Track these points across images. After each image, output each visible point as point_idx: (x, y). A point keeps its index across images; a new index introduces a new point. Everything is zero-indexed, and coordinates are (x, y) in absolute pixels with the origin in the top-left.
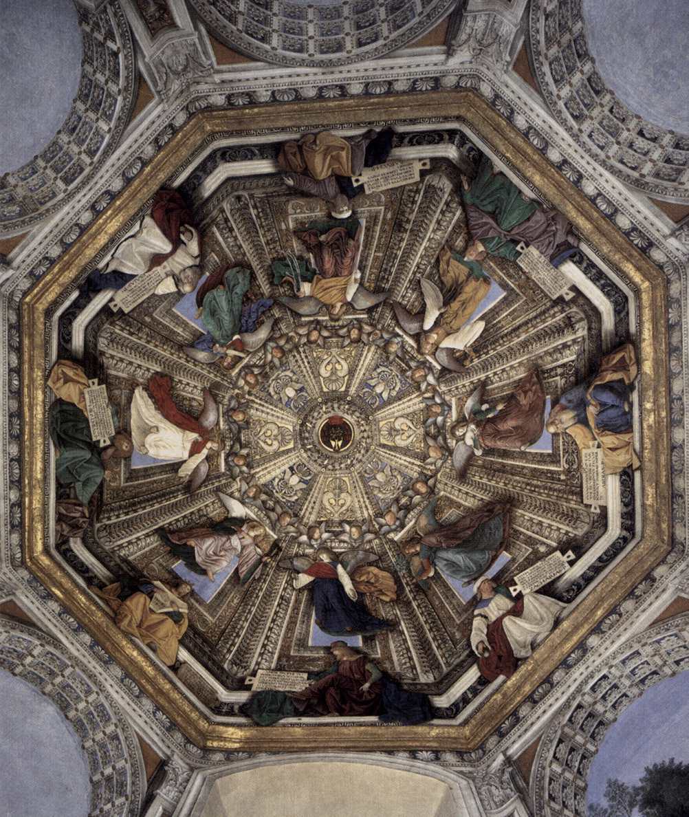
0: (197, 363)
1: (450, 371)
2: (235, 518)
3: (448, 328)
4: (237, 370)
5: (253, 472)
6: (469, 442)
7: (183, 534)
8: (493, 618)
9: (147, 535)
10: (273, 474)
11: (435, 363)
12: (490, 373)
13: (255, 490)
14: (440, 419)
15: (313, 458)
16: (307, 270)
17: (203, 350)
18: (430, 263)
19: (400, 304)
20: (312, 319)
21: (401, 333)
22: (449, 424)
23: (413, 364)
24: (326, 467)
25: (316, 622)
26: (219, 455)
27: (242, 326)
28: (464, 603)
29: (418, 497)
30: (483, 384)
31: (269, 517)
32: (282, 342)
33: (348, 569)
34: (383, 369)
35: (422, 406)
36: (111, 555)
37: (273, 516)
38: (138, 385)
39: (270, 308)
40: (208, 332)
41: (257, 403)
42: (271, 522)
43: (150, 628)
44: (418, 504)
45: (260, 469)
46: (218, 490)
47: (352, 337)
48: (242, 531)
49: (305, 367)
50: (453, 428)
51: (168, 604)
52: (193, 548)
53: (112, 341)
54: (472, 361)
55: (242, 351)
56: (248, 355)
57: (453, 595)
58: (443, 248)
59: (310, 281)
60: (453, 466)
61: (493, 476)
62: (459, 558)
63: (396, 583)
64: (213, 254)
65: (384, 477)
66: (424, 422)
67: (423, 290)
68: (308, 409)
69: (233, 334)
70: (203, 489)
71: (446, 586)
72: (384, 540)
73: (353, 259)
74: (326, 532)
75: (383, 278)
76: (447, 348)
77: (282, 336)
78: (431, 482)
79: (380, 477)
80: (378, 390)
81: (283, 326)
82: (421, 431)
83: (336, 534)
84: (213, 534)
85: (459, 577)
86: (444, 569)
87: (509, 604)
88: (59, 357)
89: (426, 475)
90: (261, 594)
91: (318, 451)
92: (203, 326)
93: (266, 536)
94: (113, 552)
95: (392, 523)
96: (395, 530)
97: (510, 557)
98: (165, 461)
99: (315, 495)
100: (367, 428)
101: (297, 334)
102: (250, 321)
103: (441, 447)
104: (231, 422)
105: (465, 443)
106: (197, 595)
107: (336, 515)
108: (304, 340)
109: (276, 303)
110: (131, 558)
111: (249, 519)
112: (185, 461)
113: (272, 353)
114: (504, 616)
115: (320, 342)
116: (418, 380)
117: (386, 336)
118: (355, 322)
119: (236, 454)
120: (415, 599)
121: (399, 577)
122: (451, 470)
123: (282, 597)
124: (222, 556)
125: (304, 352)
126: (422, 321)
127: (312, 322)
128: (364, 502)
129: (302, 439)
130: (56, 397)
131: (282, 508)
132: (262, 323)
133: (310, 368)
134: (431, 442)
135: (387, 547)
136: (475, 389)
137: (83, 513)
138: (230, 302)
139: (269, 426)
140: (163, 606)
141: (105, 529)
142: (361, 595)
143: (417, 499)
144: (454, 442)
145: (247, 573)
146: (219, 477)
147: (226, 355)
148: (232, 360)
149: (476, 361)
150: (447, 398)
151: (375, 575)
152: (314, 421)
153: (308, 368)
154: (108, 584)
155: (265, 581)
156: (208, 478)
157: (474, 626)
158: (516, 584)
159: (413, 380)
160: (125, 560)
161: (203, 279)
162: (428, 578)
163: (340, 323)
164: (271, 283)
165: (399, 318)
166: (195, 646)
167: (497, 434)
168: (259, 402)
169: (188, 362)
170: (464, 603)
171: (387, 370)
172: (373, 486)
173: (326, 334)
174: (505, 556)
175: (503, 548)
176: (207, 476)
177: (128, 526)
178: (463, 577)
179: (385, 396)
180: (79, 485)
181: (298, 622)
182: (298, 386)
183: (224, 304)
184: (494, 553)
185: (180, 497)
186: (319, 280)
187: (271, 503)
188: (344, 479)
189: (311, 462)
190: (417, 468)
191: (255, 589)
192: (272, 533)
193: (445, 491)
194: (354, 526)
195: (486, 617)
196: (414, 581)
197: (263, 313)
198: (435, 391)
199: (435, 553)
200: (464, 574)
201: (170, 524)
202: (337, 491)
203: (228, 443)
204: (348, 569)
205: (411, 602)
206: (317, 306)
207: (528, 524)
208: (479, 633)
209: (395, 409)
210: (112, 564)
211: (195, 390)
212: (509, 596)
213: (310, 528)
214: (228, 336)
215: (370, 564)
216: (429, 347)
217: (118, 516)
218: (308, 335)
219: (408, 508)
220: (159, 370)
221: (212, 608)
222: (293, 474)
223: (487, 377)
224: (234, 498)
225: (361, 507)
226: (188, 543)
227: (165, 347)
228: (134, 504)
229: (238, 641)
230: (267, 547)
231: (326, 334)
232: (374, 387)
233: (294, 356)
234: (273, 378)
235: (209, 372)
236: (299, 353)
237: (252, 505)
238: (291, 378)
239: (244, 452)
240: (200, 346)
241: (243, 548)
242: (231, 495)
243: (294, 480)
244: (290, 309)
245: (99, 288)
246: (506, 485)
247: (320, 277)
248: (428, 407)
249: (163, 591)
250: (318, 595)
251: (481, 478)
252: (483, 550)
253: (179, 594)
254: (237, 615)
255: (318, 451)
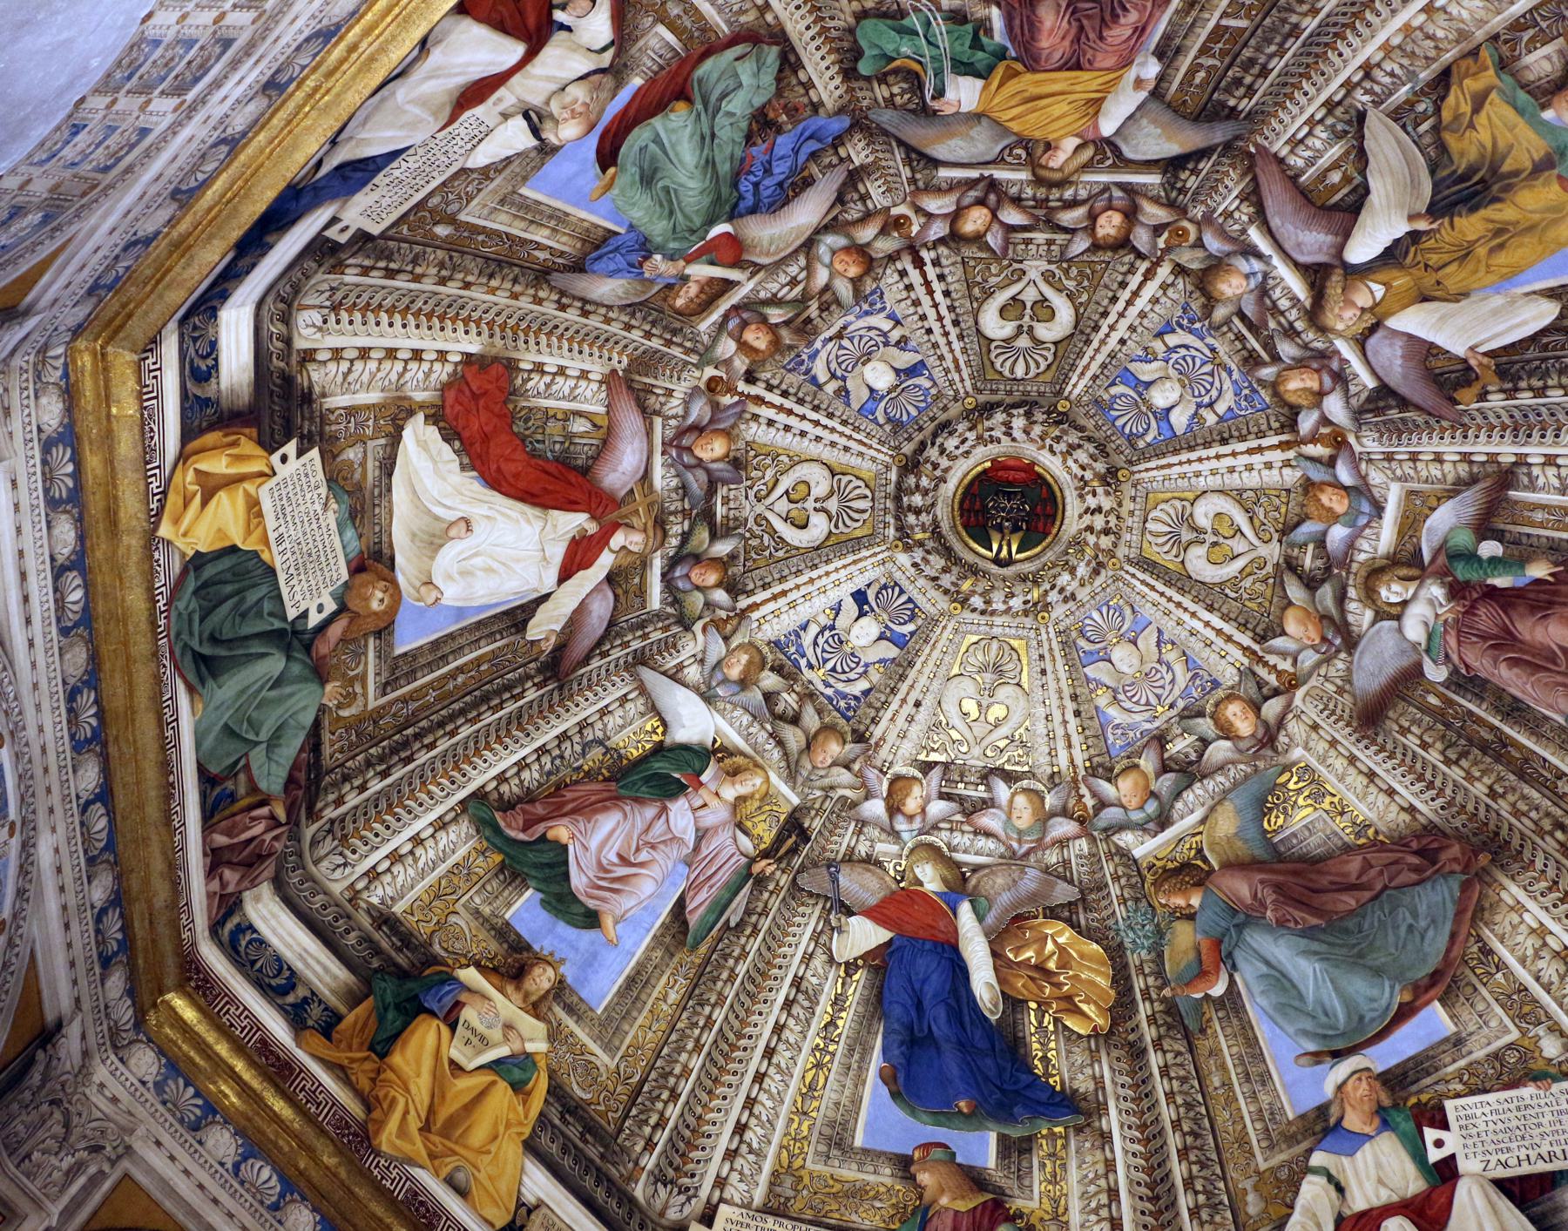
0: (588, 307)
1: (1404, 403)
2: (685, 747)
3: (1429, 280)
4: (716, 316)
5: (743, 603)
6: (1414, 630)
7: (539, 809)
8: (1359, 1202)
9: (441, 825)
10: (804, 611)
11: (1357, 365)
12: (1535, 452)
13: (744, 658)
14: (1338, 534)
15: (928, 571)
16: (976, 44)
17: (612, 274)
18: (1412, 75)
19: (1281, 161)
20: (974, 174)
21: (1264, 246)
22: (1362, 557)
23: (1287, 349)
24: (964, 602)
25: (882, 1074)
26: (644, 563)
27: (741, 197)
28: (1291, 1116)
29: (1228, 744)
30: (1506, 477)
31: (780, 743)
32: (866, 234)
33: (990, 919)
34: (1190, 339)
35: (1291, 477)
36: (349, 907)
37: (794, 737)
38: (411, 413)
39: (838, 141)
40: (631, 227)
41: (771, 405)
42: (786, 755)
43: (452, 1122)
44: (1221, 768)
45: (767, 594)
46: (641, 659)
47: (1100, 232)
48: (701, 784)
49: (936, 306)
50: (1376, 573)
51: (496, 1034)
52: (565, 848)
53: (335, 308)
54: (1483, 397)
55: (737, 264)
56: (753, 274)
57: (1265, 1078)
58: (1474, 53)
59: (983, 74)
60: (1348, 680)
61: (1464, 754)
62: (1307, 971)
63: (1115, 981)
64: (662, 30)
65: (1136, 662)
66: (1286, 530)
67: (1369, 144)
68: (930, 427)
69: (711, 222)
70: (596, 663)
71: (1252, 1042)
72: (1103, 847)
73: (1141, 31)
74: (944, 796)
75: (1238, 82)
76: (1410, 337)
77: (867, 216)
78: (1272, 708)
79: (1123, 657)
80: (1161, 397)
81: (875, 190)
82: (1272, 552)
83: (971, 809)
84: (618, 798)
85: (1291, 1030)
86: (1256, 989)
87: (1412, 1183)
88: (188, 433)
89: (1260, 684)
90: (741, 969)
91: (947, 552)
92: (615, 215)
93: (767, 796)
94: (354, 896)
95: (1135, 802)
96: (1141, 827)
97: (1450, 1028)
98: (497, 605)
99: (923, 680)
100: (1107, 503)
101: (919, 210)
102: (766, 182)
103: (1325, 618)
104: (688, 467)
105: (1400, 630)
106: (572, 991)
107: (977, 751)
108: (938, 230)
109: (861, 124)
110: (398, 908)
111: (723, 748)
112: (545, 598)
113: (830, 266)
114: (1389, 1210)
115: (994, 239)
116: (1292, 399)
117: (1214, 244)
118: (1117, 193)
119: (697, 559)
120: (1158, 1044)
121: (1126, 966)
122: (1340, 691)
123: (797, 983)
124: (642, 865)
125: (936, 263)
126: (1347, 235)
127: (971, 184)
128: (1065, 722)
129: (901, 511)
130: (183, 555)
131: (819, 712)
132: (808, 182)
133: (951, 308)
134: (1295, 591)
135: (1108, 868)
136: (1473, 480)
137: (272, 817)
138: (707, 139)
139: (802, 472)
140: (485, 1043)
141: (329, 831)
142: (1014, 1004)
143: (1220, 750)
144: (1369, 615)
145: (709, 910)
146: (642, 626)
147: (685, 279)
148: (702, 291)
149: (1496, 401)
150: (1376, 477)
151: (1061, 949)
152: (944, 462)
153: (944, 311)
154: (342, 1009)
155: (756, 930)
156: (612, 628)
157: (1300, 1202)
158: (1445, 1126)
159: (1276, 394)
160: (385, 920)
161: (624, 96)
162: (1207, 996)
163: (1068, 194)
164: (849, 73)
165: (1269, 203)
166: (565, 1150)
167: (1504, 642)
168: (778, 400)
169: (563, 308)
170: (1291, 1116)
171: (1198, 344)
172: (1099, 684)
173: (1012, 216)
174: (1435, 1020)
175: (1439, 989)
176: (612, 623)
177: (390, 806)
178: (1305, 1033)
179: (1179, 419)
180: (257, 757)
181: (835, 1067)
182: (906, 359)
183: (687, 153)
184: (1407, 997)
185: (532, 695)
186: (1012, 74)
187: (789, 700)
188: (1015, 643)
189: (921, 582)
190: (1237, 654)
191: (726, 957)
192: (784, 789)
193: (1307, 748)
194: (1025, 790)
195: (1340, 1189)
196: (1167, 992)
197: (814, 156)
198: (1338, 442)
199: (1240, 928)
200: (1308, 1025)
201: (501, 778)
202: (988, 677)
203: (676, 528)
204: (990, 919)
205: (1144, 1051)
206: (997, 142)
207: (1530, 943)
208: (1311, 1225)
209: (1205, 467)
210: (351, 940)
211: (583, 383)
212: (1419, 1155)
213: (898, 778)
214: (693, 232)
215: (1052, 913)
216: (1349, 314)
217: (363, 788)
218: (956, 217)
219: (1189, 772)
220: (474, 348)
221: (609, 1027)
222: (862, 614)
223: (1521, 461)
224: (686, 686)
225: (1050, 735)
226: (551, 835)
227: (494, 283)
228: (406, 744)
229: (673, 1112)
230: (766, 832)
231: (1012, 216)
232: (1148, 385)
233: (903, 274)
234: (827, 334)
235: (628, 327)
236: (919, 263)
237: (735, 706)
238: (885, 334)
239: (723, 548)
240: (597, 266)
241: (702, 835)
242: (675, 676)
243: (863, 633)
244: (901, 143)
245: (293, 217)
246: (1492, 794)
247: (1019, 67)
248: (1308, 486)
249: (485, 997)
250: (896, 985)
251: (1425, 746)
252: (1378, 972)
253: (526, 996)
254: (674, 1037)
255: (947, 552)
